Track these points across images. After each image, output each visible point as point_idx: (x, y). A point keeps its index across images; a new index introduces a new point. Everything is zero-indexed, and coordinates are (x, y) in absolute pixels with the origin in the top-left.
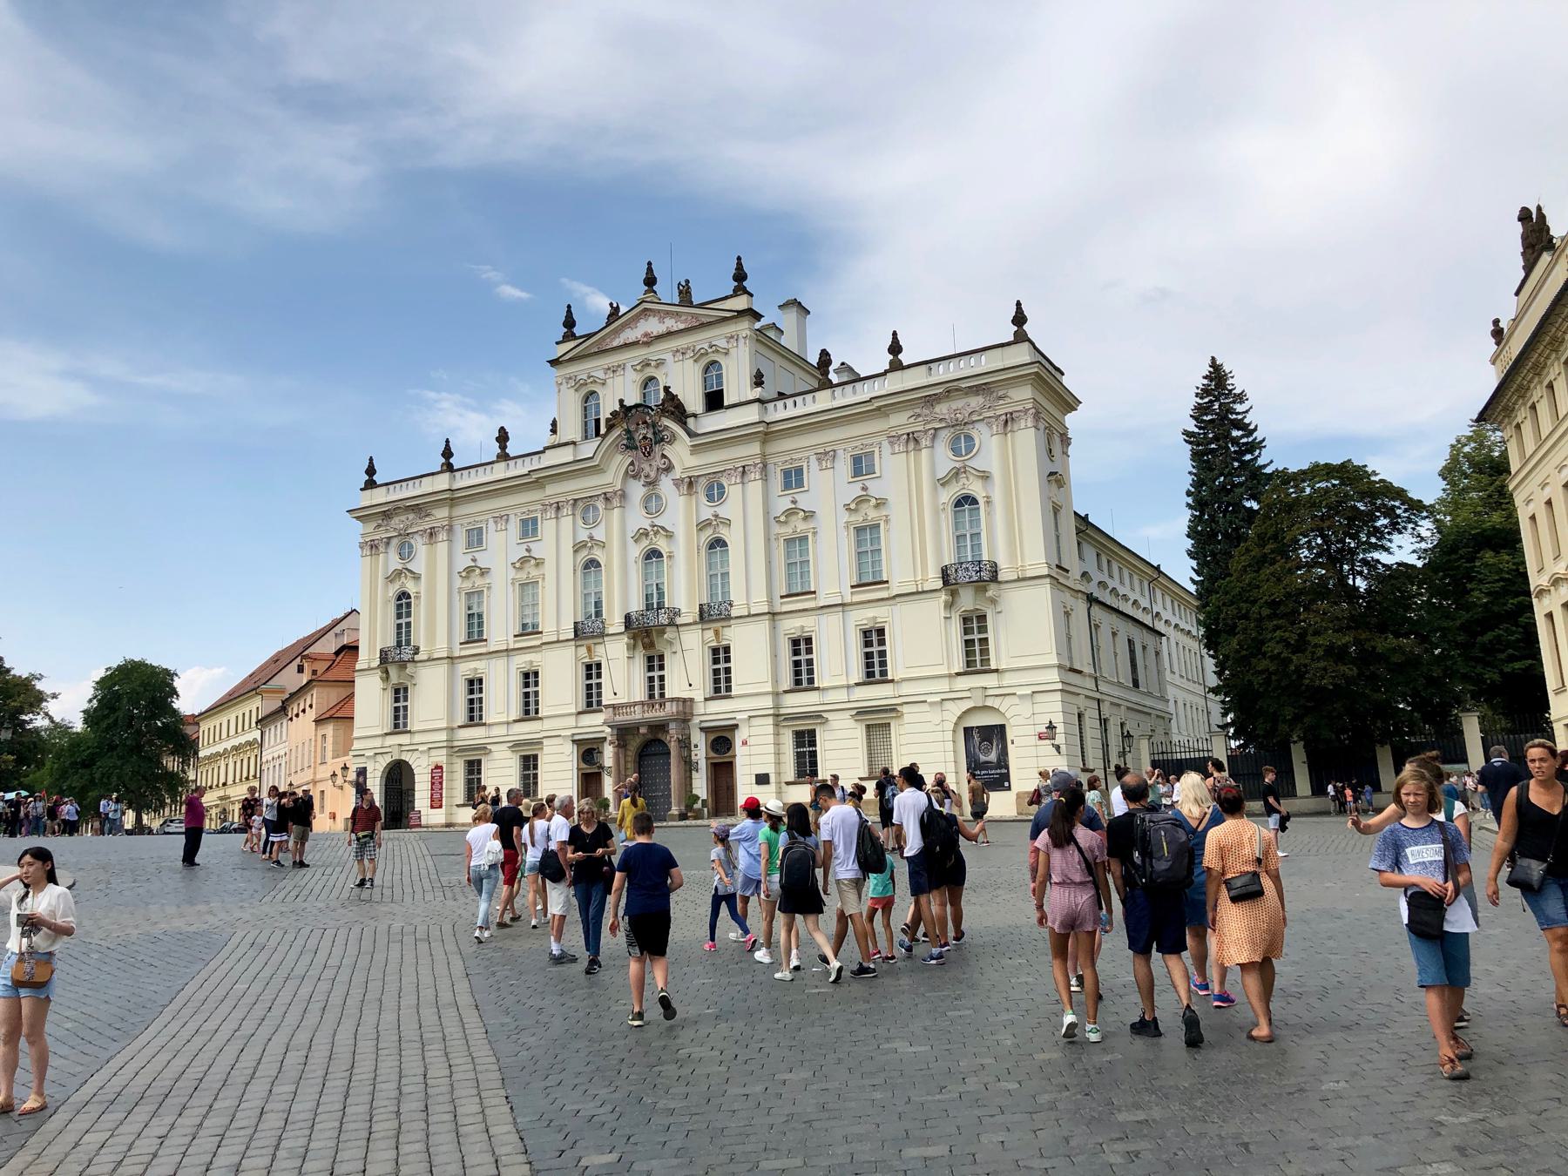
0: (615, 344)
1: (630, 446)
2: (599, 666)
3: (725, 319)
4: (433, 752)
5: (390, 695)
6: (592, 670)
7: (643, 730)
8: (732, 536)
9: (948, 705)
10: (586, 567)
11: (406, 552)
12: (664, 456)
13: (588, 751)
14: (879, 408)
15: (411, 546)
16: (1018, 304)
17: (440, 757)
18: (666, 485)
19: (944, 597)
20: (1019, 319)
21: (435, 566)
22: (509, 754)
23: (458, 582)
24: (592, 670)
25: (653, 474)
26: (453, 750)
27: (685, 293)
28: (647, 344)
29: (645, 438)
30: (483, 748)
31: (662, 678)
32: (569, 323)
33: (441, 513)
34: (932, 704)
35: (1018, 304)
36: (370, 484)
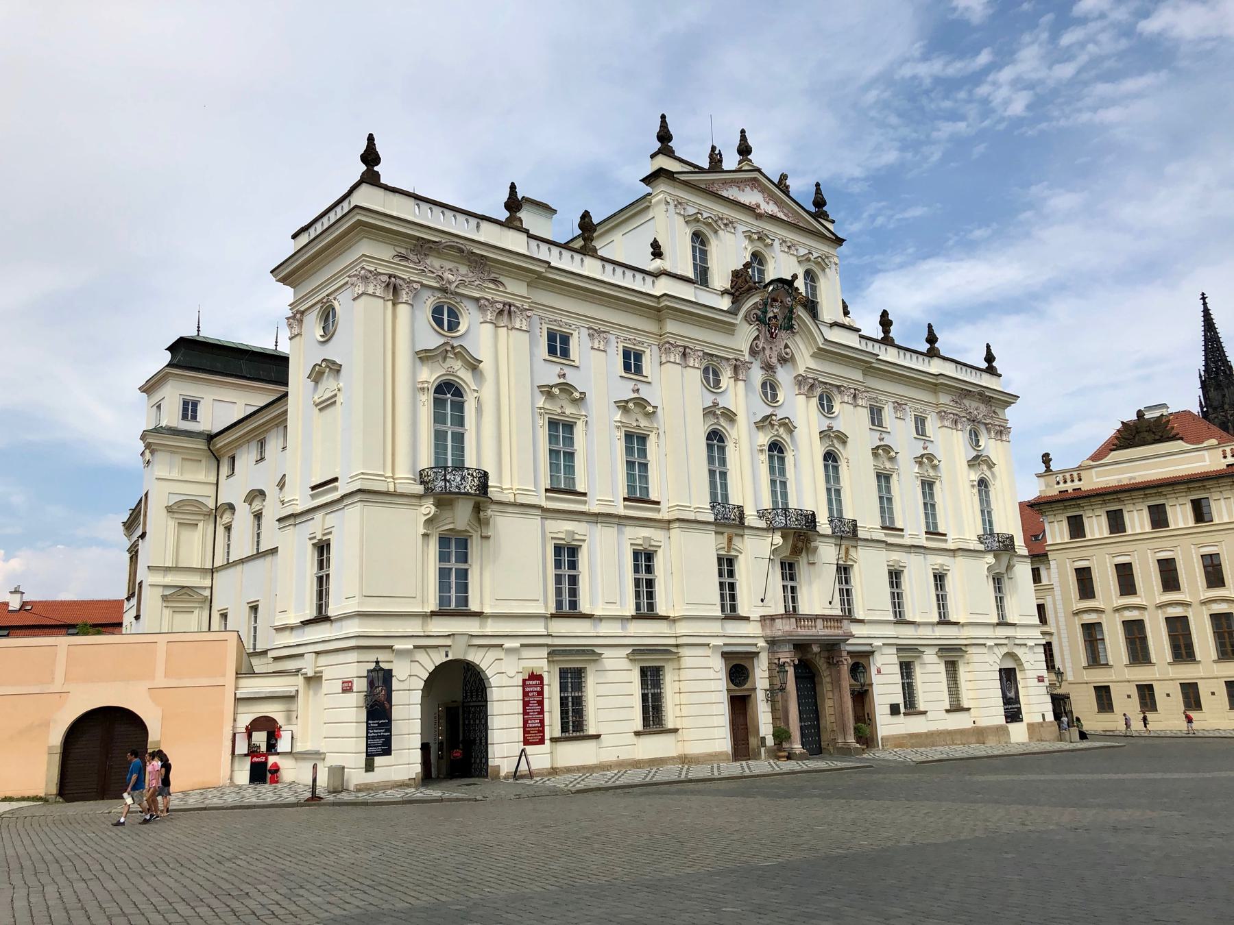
0: (725, 194)
1: (761, 319)
2: (730, 561)
3: (825, 237)
4: (527, 653)
5: (433, 548)
6: (727, 565)
7: (816, 649)
8: (844, 453)
9: (996, 650)
10: (709, 437)
11: (446, 318)
12: (786, 346)
13: (738, 669)
14: (936, 385)
15: (453, 314)
16: (988, 346)
17: (538, 662)
18: (784, 376)
19: (990, 559)
20: (990, 358)
21: (504, 357)
22: (625, 664)
23: (541, 401)
24: (727, 565)
25: (774, 360)
26: (555, 653)
27: (782, 185)
28: (759, 216)
29: (775, 317)
30: (590, 653)
31: (793, 589)
32: (664, 136)
33: (515, 288)
34: (991, 647)
35: (988, 346)
36: (371, 178)
